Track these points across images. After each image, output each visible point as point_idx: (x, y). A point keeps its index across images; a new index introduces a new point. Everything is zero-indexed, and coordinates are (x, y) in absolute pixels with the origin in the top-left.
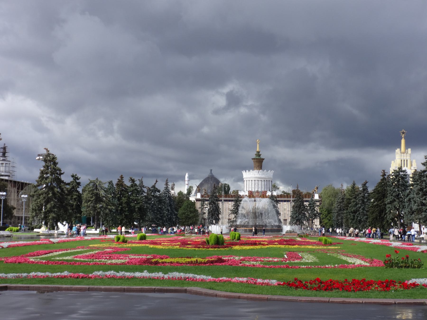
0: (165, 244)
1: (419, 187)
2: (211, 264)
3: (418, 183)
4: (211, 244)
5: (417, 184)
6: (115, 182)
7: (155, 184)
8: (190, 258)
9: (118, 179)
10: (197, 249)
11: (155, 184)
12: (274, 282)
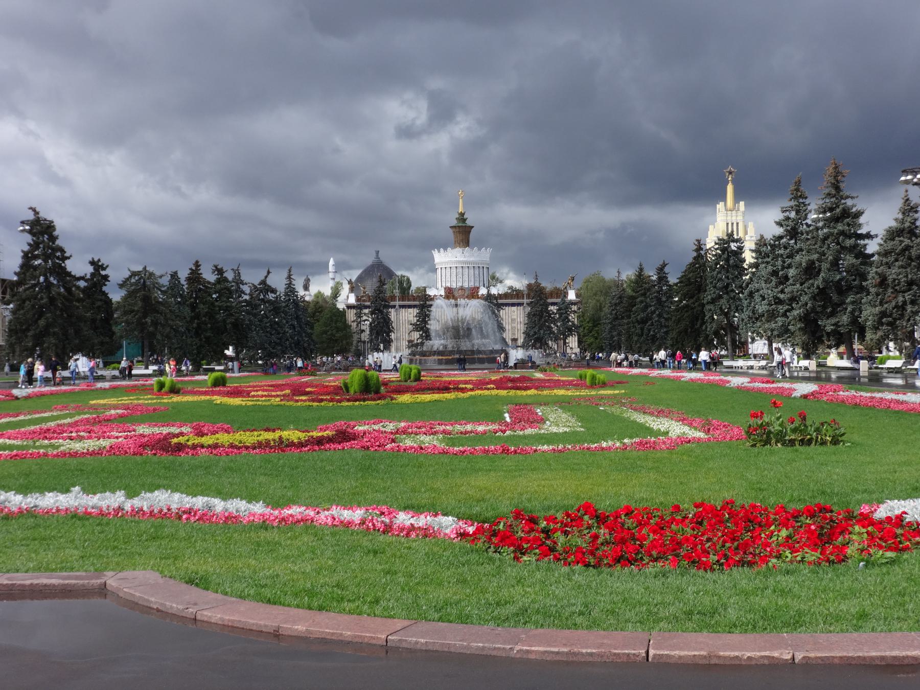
0: (260, 393)
1: (770, 268)
2: (316, 448)
3: (769, 260)
4: (352, 391)
5: (767, 263)
6: (183, 275)
7: (266, 277)
8: (274, 431)
9: (191, 269)
10: (315, 404)
11: (266, 277)
12: (448, 524)
